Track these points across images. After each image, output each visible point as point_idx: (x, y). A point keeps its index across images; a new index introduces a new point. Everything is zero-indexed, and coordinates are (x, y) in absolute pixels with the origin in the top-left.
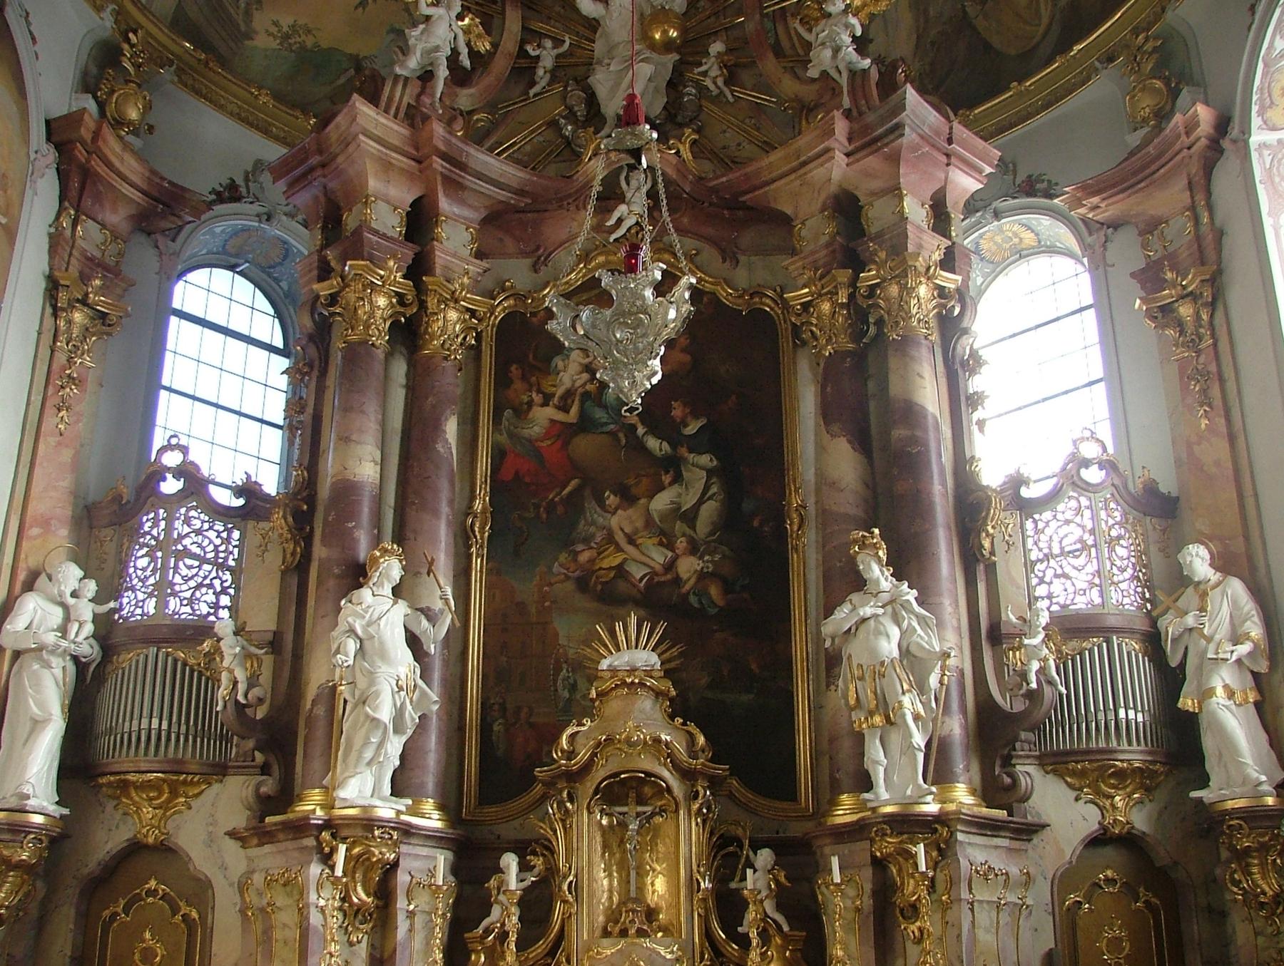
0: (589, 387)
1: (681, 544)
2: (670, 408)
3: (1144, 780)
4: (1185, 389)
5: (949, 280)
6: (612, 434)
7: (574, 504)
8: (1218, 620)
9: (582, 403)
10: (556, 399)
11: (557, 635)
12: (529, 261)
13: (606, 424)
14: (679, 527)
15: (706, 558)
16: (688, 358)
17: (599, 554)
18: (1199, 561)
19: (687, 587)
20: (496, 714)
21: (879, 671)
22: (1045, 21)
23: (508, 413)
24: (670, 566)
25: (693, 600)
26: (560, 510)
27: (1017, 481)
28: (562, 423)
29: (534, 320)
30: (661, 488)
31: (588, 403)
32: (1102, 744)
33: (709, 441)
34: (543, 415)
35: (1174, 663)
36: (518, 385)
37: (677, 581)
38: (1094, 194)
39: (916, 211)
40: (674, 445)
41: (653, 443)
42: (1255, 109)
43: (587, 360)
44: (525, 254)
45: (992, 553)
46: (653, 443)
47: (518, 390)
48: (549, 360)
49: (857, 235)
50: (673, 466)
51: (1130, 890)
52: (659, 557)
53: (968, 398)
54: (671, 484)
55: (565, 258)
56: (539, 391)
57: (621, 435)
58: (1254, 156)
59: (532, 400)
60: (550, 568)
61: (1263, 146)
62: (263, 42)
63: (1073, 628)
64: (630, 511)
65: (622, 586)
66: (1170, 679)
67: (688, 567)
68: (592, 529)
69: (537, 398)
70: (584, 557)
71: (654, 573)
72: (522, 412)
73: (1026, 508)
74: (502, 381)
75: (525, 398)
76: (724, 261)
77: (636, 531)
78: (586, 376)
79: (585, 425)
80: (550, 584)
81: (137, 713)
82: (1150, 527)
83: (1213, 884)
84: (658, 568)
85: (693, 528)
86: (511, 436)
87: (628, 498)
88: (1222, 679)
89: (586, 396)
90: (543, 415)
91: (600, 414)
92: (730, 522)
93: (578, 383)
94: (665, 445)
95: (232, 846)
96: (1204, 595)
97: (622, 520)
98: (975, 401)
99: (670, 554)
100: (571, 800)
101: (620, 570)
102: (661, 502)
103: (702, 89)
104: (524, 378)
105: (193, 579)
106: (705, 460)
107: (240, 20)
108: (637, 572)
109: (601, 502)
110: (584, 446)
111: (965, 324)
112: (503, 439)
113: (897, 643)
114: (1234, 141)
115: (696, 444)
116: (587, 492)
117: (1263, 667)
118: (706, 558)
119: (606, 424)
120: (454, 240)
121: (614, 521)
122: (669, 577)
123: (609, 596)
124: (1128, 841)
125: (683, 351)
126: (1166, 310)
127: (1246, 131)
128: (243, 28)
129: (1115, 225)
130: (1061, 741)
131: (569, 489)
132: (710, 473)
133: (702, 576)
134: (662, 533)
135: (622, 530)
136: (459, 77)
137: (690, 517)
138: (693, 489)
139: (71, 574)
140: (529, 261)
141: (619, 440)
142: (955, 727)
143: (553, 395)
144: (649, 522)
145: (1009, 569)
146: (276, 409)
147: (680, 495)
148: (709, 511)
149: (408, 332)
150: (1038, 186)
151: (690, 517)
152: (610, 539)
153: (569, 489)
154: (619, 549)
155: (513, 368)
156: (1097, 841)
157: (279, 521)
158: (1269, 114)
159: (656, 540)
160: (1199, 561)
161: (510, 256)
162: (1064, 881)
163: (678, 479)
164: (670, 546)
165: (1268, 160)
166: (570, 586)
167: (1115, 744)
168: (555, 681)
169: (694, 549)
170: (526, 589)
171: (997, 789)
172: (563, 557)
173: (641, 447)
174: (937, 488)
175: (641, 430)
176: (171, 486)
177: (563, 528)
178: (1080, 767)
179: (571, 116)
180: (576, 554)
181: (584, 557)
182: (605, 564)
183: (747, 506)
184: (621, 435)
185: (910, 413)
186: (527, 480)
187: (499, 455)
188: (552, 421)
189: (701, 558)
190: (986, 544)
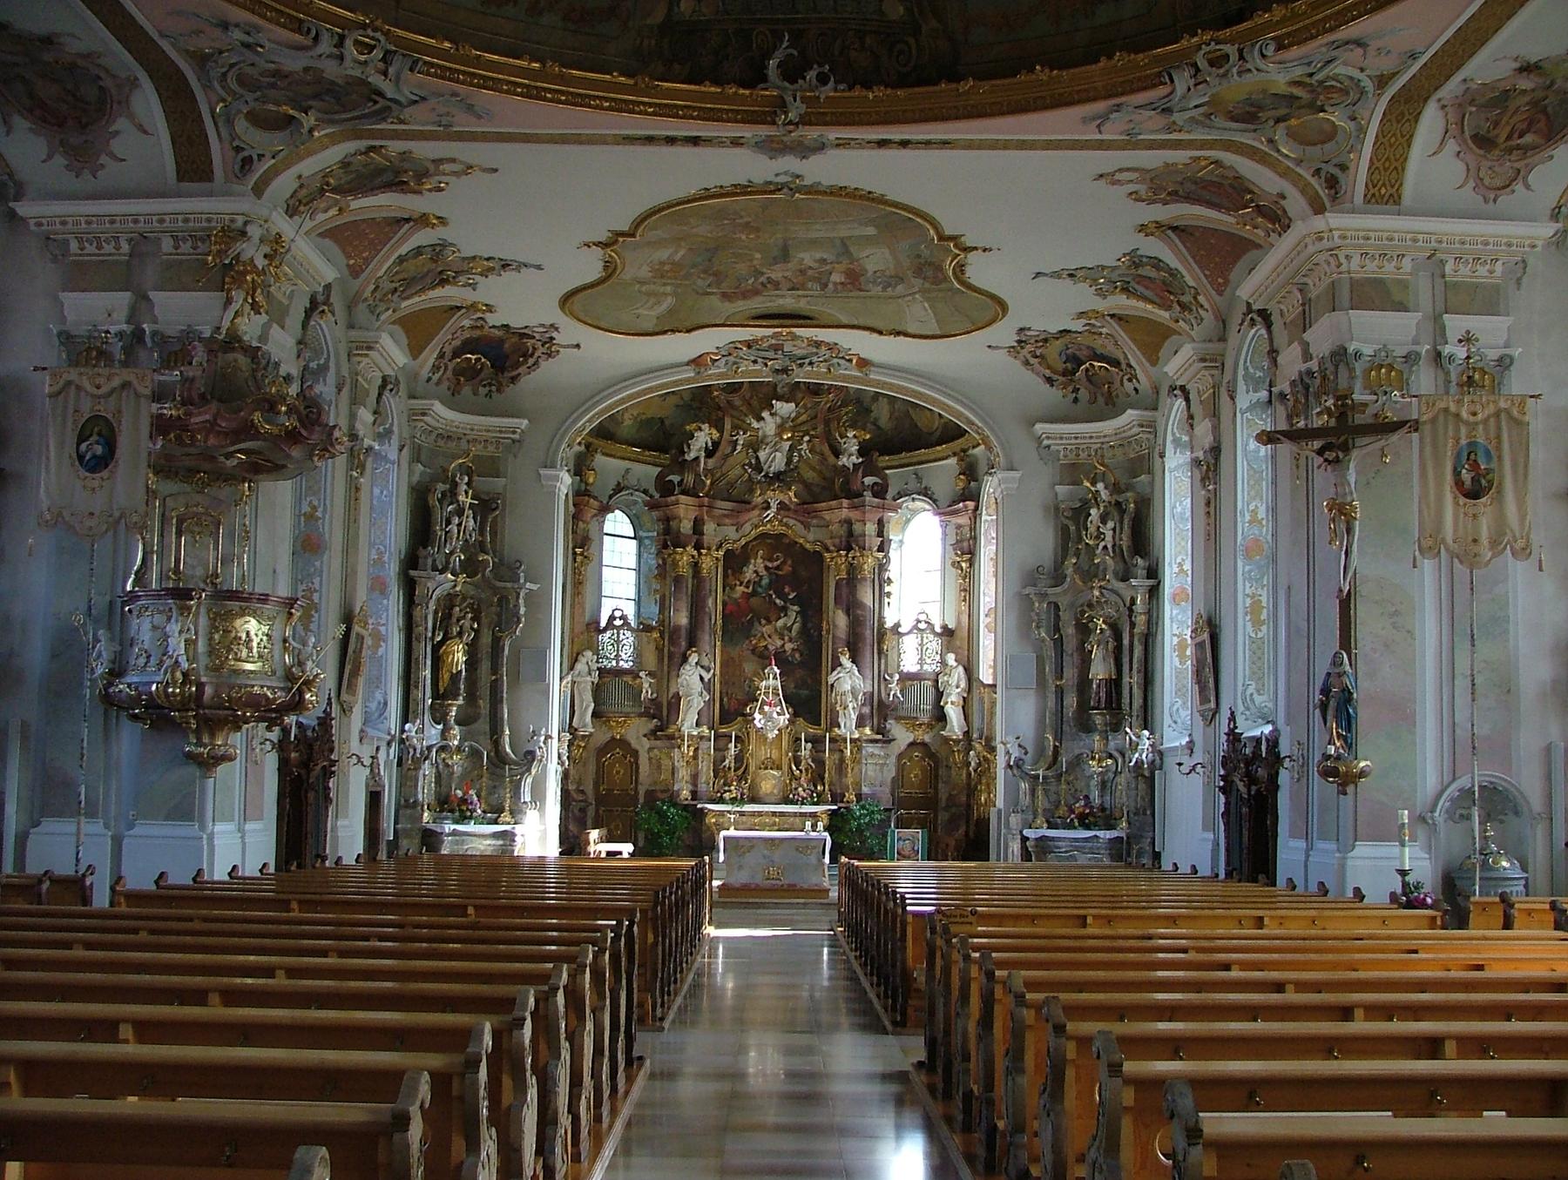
3: (930, 726)
5: (881, 555)
7: (751, 622)
8: (953, 681)
18: (951, 659)
21: (844, 694)
27: (898, 625)
39: (871, 528)
47: (731, 580)
49: (851, 541)
50: (784, 609)
52: (779, 643)
55: (747, 527)
62: (628, 422)
63: (906, 678)
66: (939, 695)
67: (789, 646)
72: (732, 588)
73: (901, 635)
74: (725, 576)
79: (755, 593)
87: (769, 621)
88: (953, 698)
90: (740, 589)
92: (804, 631)
97: (767, 629)
98: (889, 595)
102: (780, 623)
103: (800, 456)
105: (623, 651)
110: (753, 600)
113: (848, 682)
123: (763, 657)
124: (924, 744)
130: (902, 713)
136: (710, 454)
138: (791, 619)
139: (589, 654)
142: (866, 710)
145: (892, 655)
146: (633, 563)
149: (696, 566)
156: (912, 744)
157: (656, 635)
162: (900, 756)
169: (790, 640)
170: (734, 652)
171: (880, 730)
174: (868, 632)
176: (618, 623)
178: (910, 722)
179: (750, 465)
185: (861, 605)
187: (724, 604)
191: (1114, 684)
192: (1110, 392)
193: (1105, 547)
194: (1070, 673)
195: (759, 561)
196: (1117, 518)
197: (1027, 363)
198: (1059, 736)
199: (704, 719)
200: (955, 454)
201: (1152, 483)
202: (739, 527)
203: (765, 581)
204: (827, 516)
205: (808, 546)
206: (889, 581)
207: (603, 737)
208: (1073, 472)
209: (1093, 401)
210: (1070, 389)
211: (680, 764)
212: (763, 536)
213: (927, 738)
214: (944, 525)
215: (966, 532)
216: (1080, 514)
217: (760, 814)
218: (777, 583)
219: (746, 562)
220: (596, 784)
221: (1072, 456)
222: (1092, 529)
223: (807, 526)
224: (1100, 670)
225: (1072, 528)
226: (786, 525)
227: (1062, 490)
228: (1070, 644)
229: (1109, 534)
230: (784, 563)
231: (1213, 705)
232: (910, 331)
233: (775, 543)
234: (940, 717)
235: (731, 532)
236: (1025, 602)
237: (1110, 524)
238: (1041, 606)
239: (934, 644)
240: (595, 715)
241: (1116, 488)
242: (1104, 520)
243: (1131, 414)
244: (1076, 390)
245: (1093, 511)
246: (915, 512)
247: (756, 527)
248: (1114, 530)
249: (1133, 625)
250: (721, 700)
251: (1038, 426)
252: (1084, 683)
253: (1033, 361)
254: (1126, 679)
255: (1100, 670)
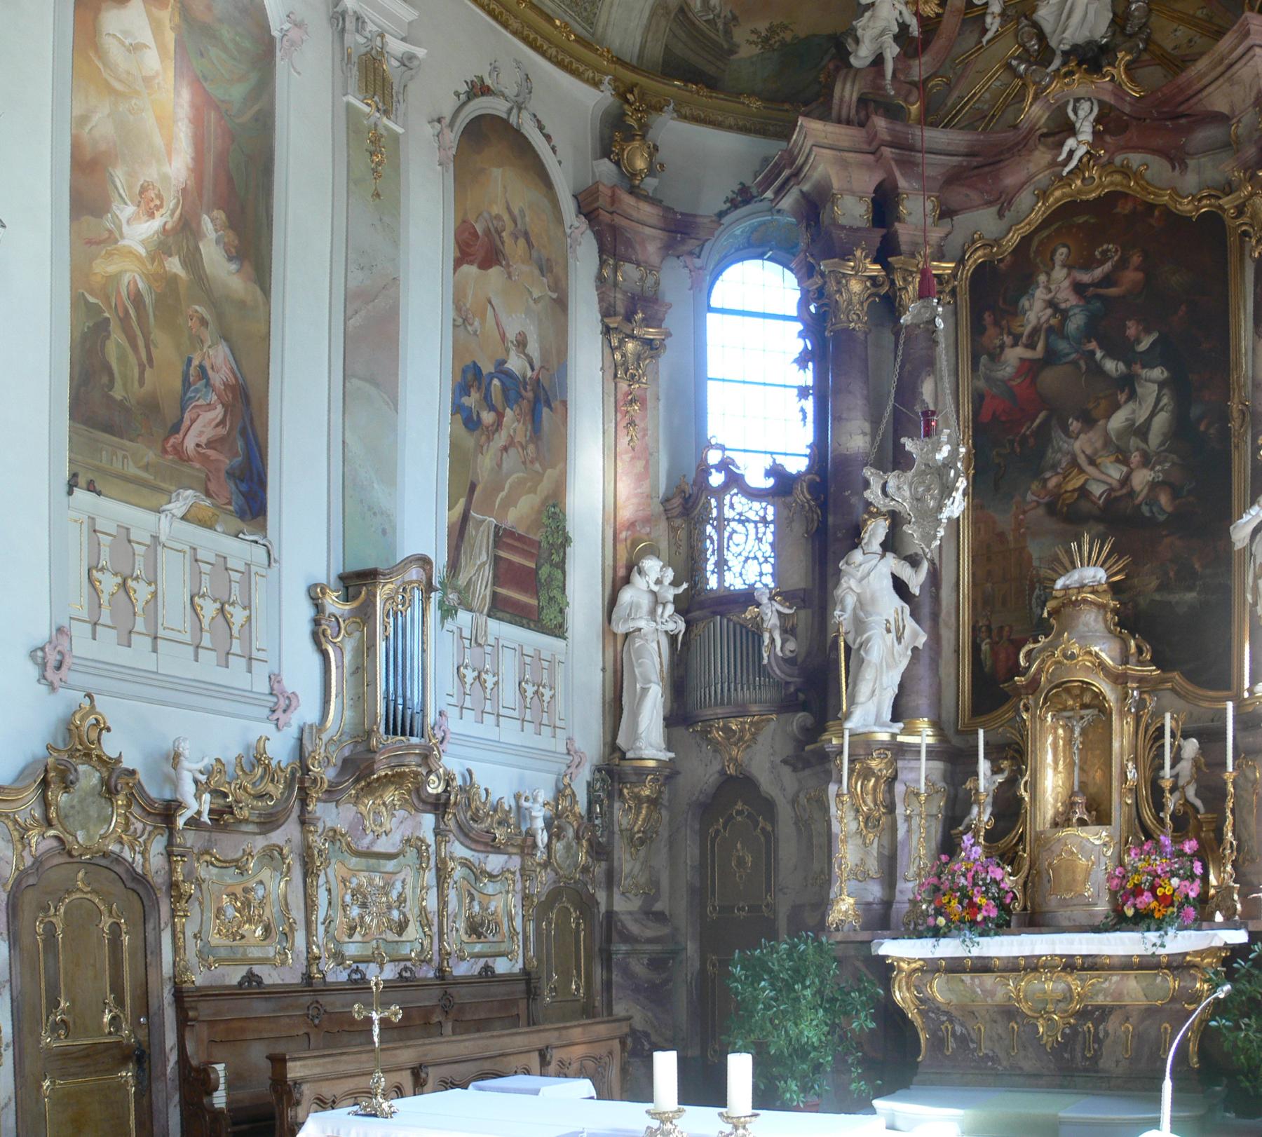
0: (1053, 321)
1: (1135, 458)
2: (1124, 327)
6: (1074, 363)
7: (1043, 435)
9: (1047, 338)
10: (1024, 339)
11: (1030, 558)
12: (994, 209)
13: (1068, 354)
14: (1134, 442)
15: (1158, 468)
16: (1139, 276)
17: (1065, 478)
19: (1140, 498)
20: (983, 635)
23: (984, 359)
24: (1125, 481)
25: (1145, 509)
26: (1031, 441)
28: (1030, 360)
29: (1001, 265)
30: (1116, 407)
31: (1052, 337)
33: (1163, 353)
34: (1013, 355)
36: (991, 331)
37: (1132, 494)
40: (1129, 364)
41: (1110, 366)
43: (1049, 297)
44: (989, 203)
46: (1110, 366)
47: (992, 337)
48: (1017, 301)
50: (1128, 384)
52: (1115, 473)
54: (1126, 402)
55: (1025, 199)
56: (1009, 333)
57: (1082, 363)
59: (1004, 343)
60: (1024, 497)
62: (747, 51)
64: (1091, 434)
65: (1085, 506)
67: (1141, 478)
68: (1059, 456)
69: (1008, 340)
70: (1052, 483)
71: (1112, 489)
72: (995, 356)
74: (977, 328)
75: (997, 342)
76: (1174, 168)
77: (1096, 452)
78: (1049, 311)
79: (1051, 357)
80: (1024, 512)
81: (716, 663)
84: (1115, 484)
85: (1146, 441)
86: (988, 379)
87: (1089, 421)
89: (1050, 330)
90: (1013, 355)
91: (1062, 346)
92: (1181, 429)
93: (1043, 319)
94: (1121, 366)
95: (786, 770)
97: (1083, 444)
99: (1125, 469)
100: (1027, 710)
101: (1083, 492)
102: (1117, 421)
104: (996, 323)
106: (1158, 373)
107: (721, 39)
108: (1097, 490)
109: (1065, 429)
110: (1050, 378)
112: (981, 384)
115: (1148, 360)
116: (1054, 422)
118: (1158, 468)
119: (1068, 354)
120: (915, 210)
121: (1077, 445)
122: (1124, 491)
123: (1072, 515)
125: (1137, 269)
128: (726, 46)
131: (1038, 421)
132: (1162, 385)
133: (1153, 486)
134: (1119, 450)
135: (1083, 452)
137: (1142, 432)
138: (1148, 406)
140: (994, 209)
141: (1079, 368)
143: (1021, 335)
144: (1107, 442)
147: (1134, 412)
148: (1161, 421)
151: (1142, 432)
152: (1074, 463)
153: (1038, 421)
154: (1082, 471)
155: (986, 315)
159: (1113, 458)
161: (977, 207)
163: (1132, 395)
164: (1125, 461)
166: (1041, 511)
168: (1030, 600)
169: (1146, 462)
170: (1004, 521)
172: (1035, 486)
173: (1099, 370)
175: (1099, 355)
177: (1033, 458)
180: (1045, 481)
181: (1052, 483)
182: (1070, 487)
183: (1195, 411)
184: (1082, 363)
186: (1003, 419)
188: (1021, 359)
189: (1152, 469)
195: (1059, 273)
199: (922, 700)
202: (1003, 202)
203: (1076, 322)
204: (1218, 100)
205: (1185, 206)
207: (703, 773)
211: (844, 822)
212: (1070, 209)
217: (1032, 965)
218: (1105, 323)
219: (1026, 283)
220: (699, 894)
223: (1177, 159)
226: (1125, 171)
230: (1122, 264)
233: (1088, 223)
235: (984, 221)
240: (679, 717)
247: (1043, 195)
250: (976, 648)
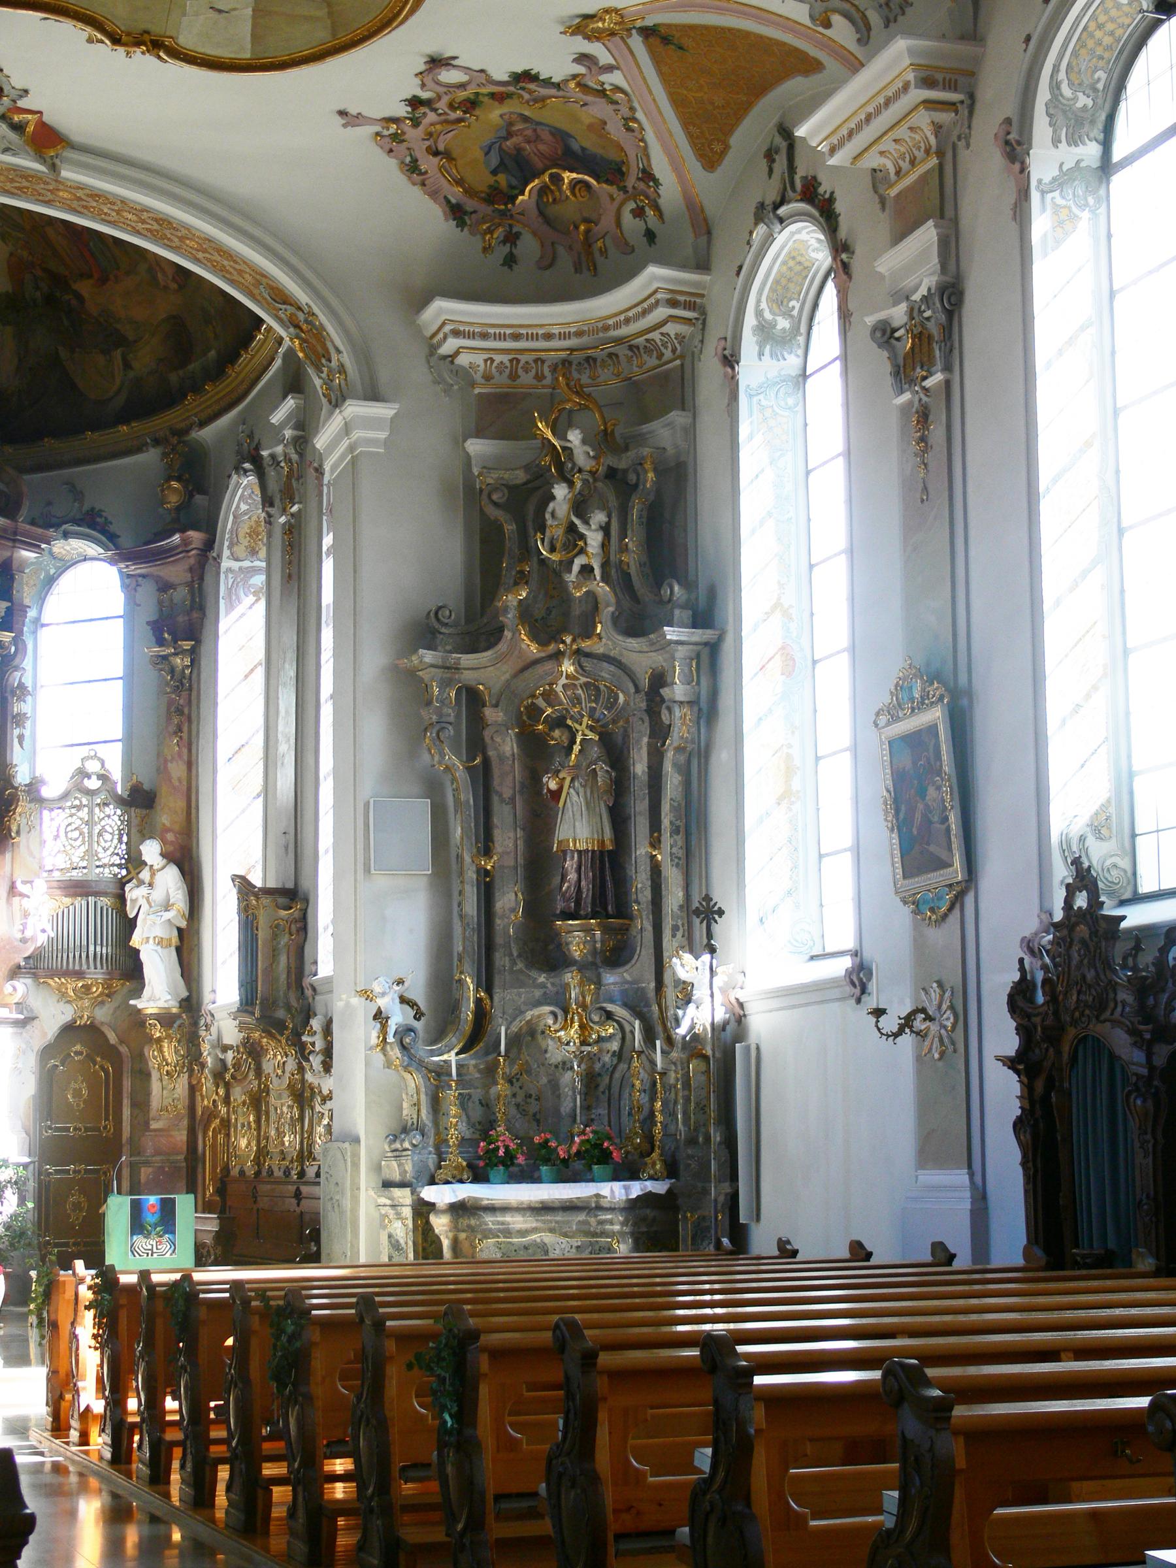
4: (169, 719)
18: (151, 851)
22: (118, 382)
32: (77, 968)
35: (131, 916)
38: (129, 560)
42: (226, 544)
45: (18, 833)
51: (90, 1058)
53: (14, 717)
58: (222, 576)
61: (229, 570)
66: (128, 925)
82: (133, 814)
83: (140, 1057)
96: (153, 875)
111: (16, 662)
114: (215, 559)
117: (183, 924)
126: (165, 658)
127: (219, 556)
129: (144, 576)
150: (98, 520)
156: (69, 1030)
158: (235, 549)
160: (151, 851)
165: (231, 581)
167: (85, 967)
190: (14, 828)
191: (610, 863)
192: (588, 244)
193: (587, 570)
194: (508, 840)
196: (613, 502)
197: (412, 168)
198: (487, 983)
200: (157, 442)
201: (691, 432)
206: (22, 691)
208: (500, 407)
209: (548, 262)
210: (499, 232)
213: (102, 1015)
214: (130, 584)
215: (181, 594)
216: (527, 499)
221: (503, 379)
222: (555, 529)
224: (578, 828)
225: (510, 528)
227: (476, 447)
228: (508, 780)
229: (594, 539)
231: (957, 871)
232: (187, 40)
234: (130, 970)
236: (409, 688)
237: (599, 517)
238: (445, 696)
239: (112, 818)
241: (604, 441)
242: (580, 507)
243: (655, 276)
244: (511, 238)
245: (560, 491)
246: (66, 565)
248: (606, 529)
249: (660, 732)
251: (442, 309)
252: (539, 861)
253: (429, 164)
254: (641, 849)
255: (578, 828)
